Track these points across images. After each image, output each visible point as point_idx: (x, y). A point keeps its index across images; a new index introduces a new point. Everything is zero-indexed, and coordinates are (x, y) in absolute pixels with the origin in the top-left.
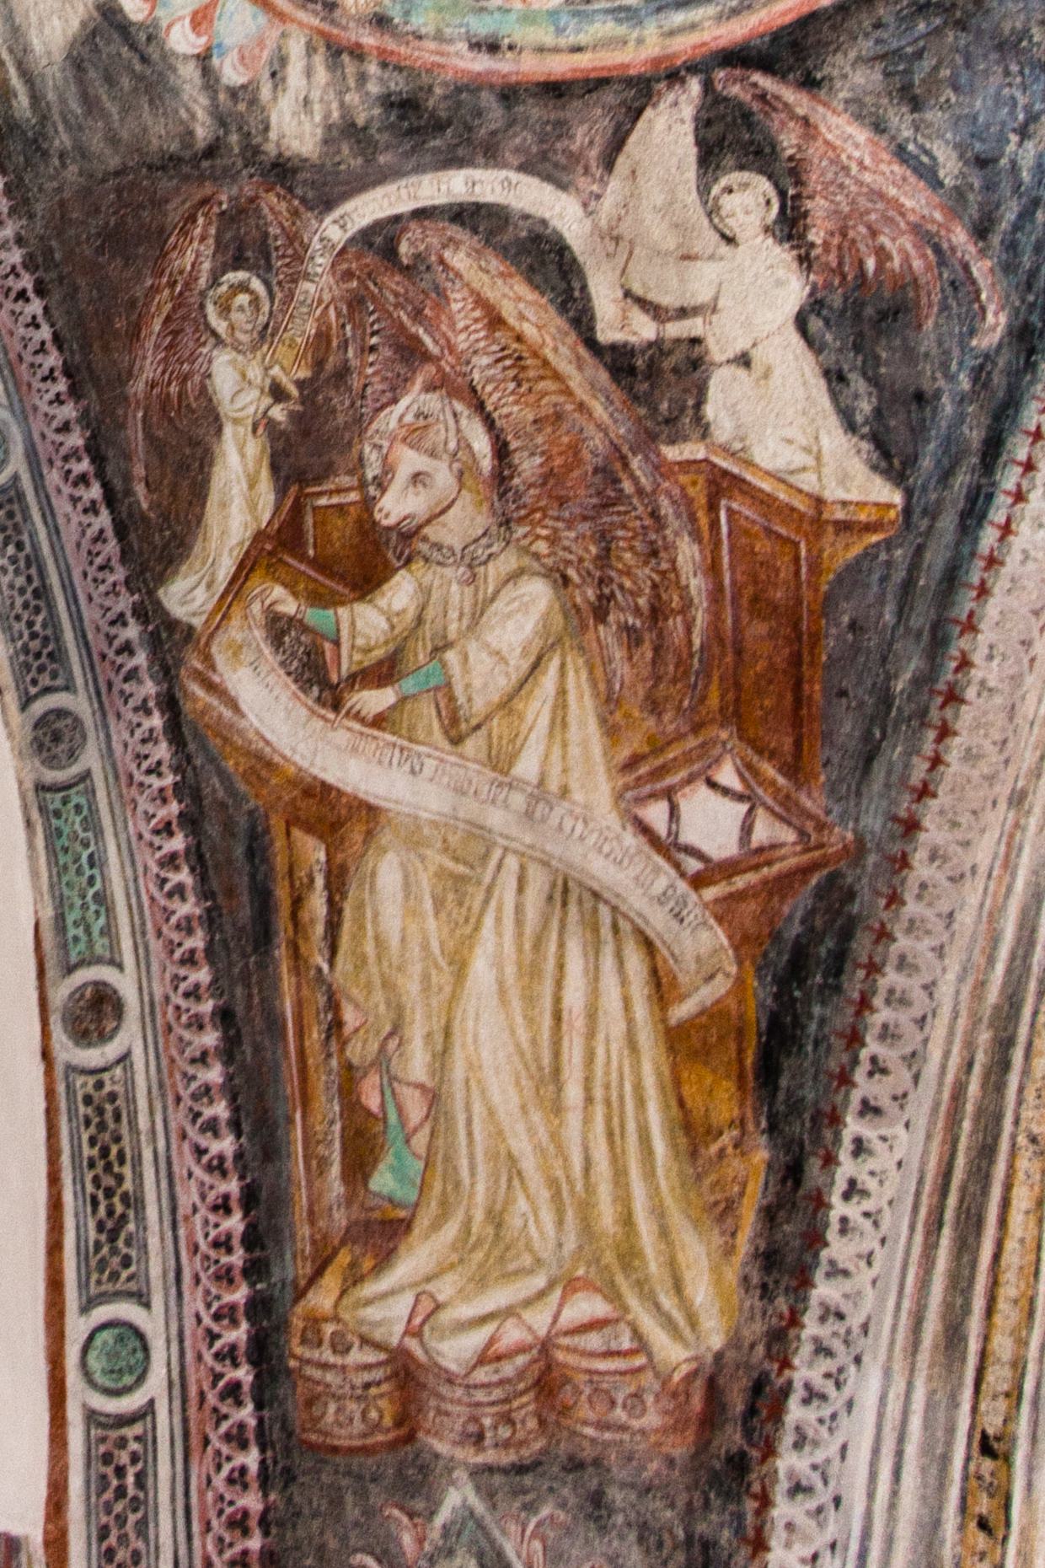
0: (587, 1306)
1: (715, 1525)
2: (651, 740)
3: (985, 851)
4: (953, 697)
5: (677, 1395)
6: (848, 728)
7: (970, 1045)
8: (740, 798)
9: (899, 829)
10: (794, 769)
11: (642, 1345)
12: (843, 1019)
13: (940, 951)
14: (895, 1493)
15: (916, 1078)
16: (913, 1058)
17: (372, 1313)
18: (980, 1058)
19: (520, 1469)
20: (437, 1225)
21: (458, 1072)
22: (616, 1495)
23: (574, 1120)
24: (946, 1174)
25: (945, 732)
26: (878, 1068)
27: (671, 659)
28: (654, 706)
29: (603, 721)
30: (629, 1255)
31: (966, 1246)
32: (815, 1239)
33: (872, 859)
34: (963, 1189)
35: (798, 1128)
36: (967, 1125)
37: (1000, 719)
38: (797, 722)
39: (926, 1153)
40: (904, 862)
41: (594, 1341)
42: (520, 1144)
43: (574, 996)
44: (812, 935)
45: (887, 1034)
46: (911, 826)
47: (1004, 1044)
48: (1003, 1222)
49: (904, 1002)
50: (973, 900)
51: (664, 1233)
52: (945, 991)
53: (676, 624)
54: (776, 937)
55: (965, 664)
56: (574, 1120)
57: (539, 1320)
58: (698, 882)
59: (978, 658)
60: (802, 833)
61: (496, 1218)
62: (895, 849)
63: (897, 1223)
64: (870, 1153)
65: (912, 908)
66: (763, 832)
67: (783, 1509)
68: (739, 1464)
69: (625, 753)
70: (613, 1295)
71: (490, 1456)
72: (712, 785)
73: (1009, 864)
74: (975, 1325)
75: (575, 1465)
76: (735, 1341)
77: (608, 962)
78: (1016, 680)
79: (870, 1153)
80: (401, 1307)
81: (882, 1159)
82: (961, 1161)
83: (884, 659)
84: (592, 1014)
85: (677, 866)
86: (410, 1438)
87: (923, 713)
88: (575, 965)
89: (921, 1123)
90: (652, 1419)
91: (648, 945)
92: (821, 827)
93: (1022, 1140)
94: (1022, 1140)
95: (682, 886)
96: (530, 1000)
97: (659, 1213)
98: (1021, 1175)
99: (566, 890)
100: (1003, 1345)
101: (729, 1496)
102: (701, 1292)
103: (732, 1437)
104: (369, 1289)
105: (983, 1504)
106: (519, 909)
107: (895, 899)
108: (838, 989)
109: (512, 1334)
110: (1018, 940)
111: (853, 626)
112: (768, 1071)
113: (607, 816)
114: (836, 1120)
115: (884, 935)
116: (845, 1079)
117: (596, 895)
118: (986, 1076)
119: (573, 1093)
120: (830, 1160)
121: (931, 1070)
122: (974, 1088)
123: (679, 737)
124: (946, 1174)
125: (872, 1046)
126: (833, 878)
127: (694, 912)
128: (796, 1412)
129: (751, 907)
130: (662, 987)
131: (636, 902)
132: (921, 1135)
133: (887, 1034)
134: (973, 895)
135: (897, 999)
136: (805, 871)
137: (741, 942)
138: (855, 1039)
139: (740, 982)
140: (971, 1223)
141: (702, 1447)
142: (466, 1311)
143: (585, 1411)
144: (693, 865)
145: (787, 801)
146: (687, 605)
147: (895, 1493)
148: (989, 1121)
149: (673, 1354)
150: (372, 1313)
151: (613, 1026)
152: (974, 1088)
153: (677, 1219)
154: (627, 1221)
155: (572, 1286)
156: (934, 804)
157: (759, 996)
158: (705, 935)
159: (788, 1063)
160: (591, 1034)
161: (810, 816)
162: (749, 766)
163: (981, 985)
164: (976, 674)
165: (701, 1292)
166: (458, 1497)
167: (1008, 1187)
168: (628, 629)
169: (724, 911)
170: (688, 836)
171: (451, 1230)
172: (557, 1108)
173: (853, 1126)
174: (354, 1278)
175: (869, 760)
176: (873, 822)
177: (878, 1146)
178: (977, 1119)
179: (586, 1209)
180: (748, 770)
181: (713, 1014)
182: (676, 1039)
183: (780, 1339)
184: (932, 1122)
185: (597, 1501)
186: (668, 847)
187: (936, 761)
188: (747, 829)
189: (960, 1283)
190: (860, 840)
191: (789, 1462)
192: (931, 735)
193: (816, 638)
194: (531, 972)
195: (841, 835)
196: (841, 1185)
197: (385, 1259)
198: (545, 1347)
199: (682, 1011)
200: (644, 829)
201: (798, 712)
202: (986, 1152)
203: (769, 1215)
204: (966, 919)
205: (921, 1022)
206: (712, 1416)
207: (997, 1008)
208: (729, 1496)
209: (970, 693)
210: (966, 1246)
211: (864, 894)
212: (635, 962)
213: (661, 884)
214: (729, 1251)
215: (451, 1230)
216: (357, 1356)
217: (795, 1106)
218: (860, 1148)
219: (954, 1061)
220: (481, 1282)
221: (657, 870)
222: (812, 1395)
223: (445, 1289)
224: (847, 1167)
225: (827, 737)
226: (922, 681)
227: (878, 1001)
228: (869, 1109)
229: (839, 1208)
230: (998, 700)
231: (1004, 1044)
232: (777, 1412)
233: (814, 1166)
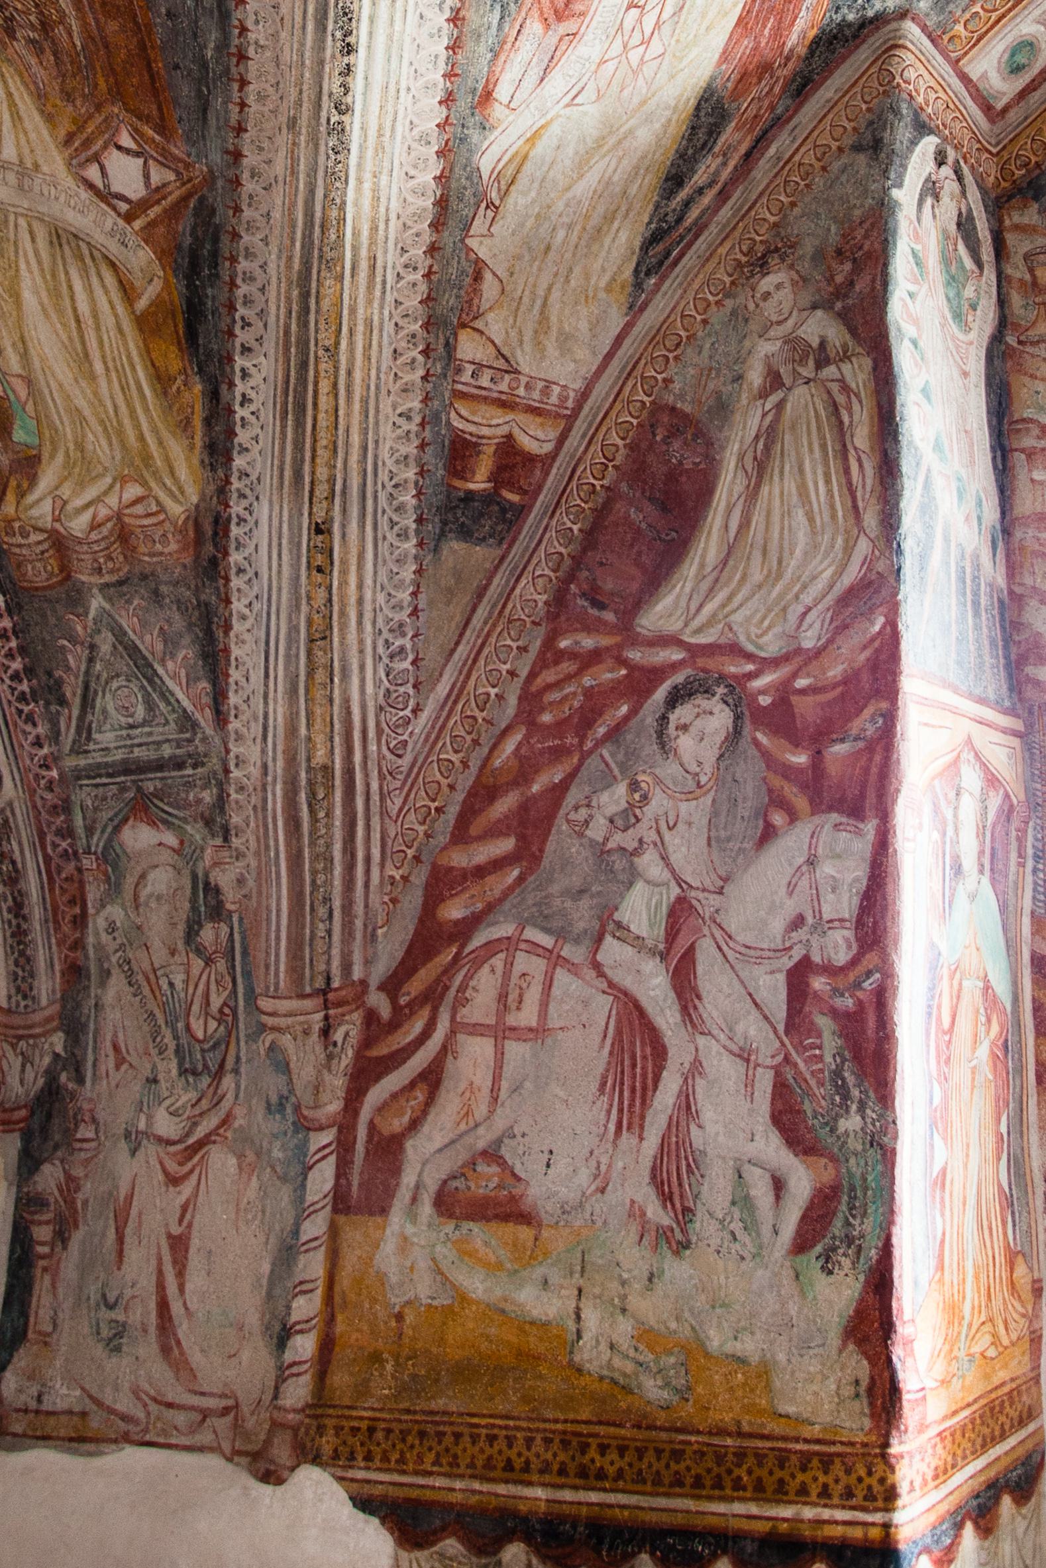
0: (133, 491)
1: (208, 595)
2: (74, 121)
3: (280, 167)
4: (242, 57)
5: (182, 531)
6: (186, 90)
7: (289, 299)
8: (137, 154)
9: (230, 159)
10: (162, 129)
11: (162, 509)
12: (223, 297)
13: (265, 241)
14: (280, 565)
15: (265, 325)
16: (262, 314)
17: (35, 512)
18: (295, 307)
19: (121, 583)
20: (52, 457)
21: (37, 364)
22: (164, 589)
23: (103, 383)
24: (287, 382)
25: (243, 83)
26: (246, 324)
27: (66, 59)
28: (68, 96)
29: (42, 112)
30: (147, 459)
31: (299, 424)
32: (231, 433)
33: (220, 183)
34: (295, 390)
35: (212, 369)
36: (293, 350)
37: (270, 68)
38: (155, 92)
39: (276, 370)
40: (237, 182)
41: (139, 509)
42: (81, 402)
43: (83, 307)
44: (198, 242)
45: (247, 301)
46: (237, 155)
47: (305, 296)
48: (315, 405)
49: (252, 279)
50: (279, 202)
51: (160, 443)
52: (272, 268)
53: (60, 31)
54: (179, 247)
55: (244, 30)
56: (103, 383)
57: (113, 501)
58: (129, 218)
59: (250, 24)
60: (178, 173)
61: (80, 447)
62: (230, 174)
63: (267, 415)
64: (250, 376)
65: (247, 213)
66: (158, 176)
67: (236, 582)
68: (214, 562)
69: (62, 133)
70: (144, 484)
71: (107, 578)
72: (119, 148)
73: (294, 172)
74: (307, 468)
75: (144, 577)
76: (203, 497)
77: (95, 280)
78: (275, 36)
79: (250, 376)
80: (46, 507)
81: (256, 379)
82: (293, 373)
83: (195, 35)
84: (95, 315)
85: (114, 209)
86: (68, 577)
87: (227, 71)
88: (78, 286)
89: (272, 352)
90: (173, 546)
91: (113, 265)
92: (187, 166)
93: (321, 353)
94: (321, 353)
95: (121, 222)
96: (60, 312)
97: (155, 430)
98: (323, 374)
99: (58, 237)
100: (322, 473)
101: (213, 579)
102: (183, 473)
103: (209, 549)
104: (31, 498)
105: (319, 560)
106: (37, 253)
107: (237, 210)
108: (217, 276)
109: (103, 512)
110: (305, 224)
111: (170, 15)
112: (192, 335)
113: (69, 182)
114: (230, 360)
115: (236, 236)
116: (231, 334)
117: (75, 236)
118: (299, 318)
119: (99, 367)
120: (231, 385)
121: (272, 319)
122: (294, 327)
123: (91, 117)
124: (287, 382)
125: (241, 311)
126: (202, 199)
127: (132, 240)
128: (235, 531)
129: (161, 230)
130: (128, 292)
131: (99, 238)
132: (273, 360)
133: (247, 301)
134: (278, 198)
135: (249, 278)
136: (185, 199)
137: (161, 255)
138: (232, 308)
139: (166, 281)
140: (301, 408)
141: (197, 557)
142: (78, 502)
143: (142, 549)
144: (124, 207)
145: (164, 152)
146: (63, 16)
147: (280, 565)
148: (303, 344)
149: (176, 510)
150: (35, 512)
151: (108, 321)
152: (294, 327)
153: (165, 434)
154: (141, 438)
155: (123, 480)
156: (246, 136)
157: (179, 287)
158: (141, 253)
159: (201, 329)
160: (98, 329)
161: (181, 160)
162: (136, 130)
163: (290, 258)
164: (252, 36)
165: (183, 473)
166: (97, 603)
167: (316, 384)
168: (32, 41)
169: (147, 234)
170: (116, 188)
171: (60, 458)
172: (93, 377)
173: (240, 362)
174: (21, 495)
175: (205, 111)
176: (216, 157)
177: (253, 371)
178: (297, 347)
179: (120, 433)
180: (136, 133)
181: (156, 303)
182: (141, 321)
183: (222, 491)
184: (277, 352)
185: (156, 592)
186: (106, 196)
187: (243, 105)
188: (147, 176)
189: (298, 446)
190: (211, 171)
191: (235, 557)
192: (236, 86)
193: (149, 26)
194: (55, 293)
195: (201, 168)
196: (239, 398)
197: (33, 480)
198: (119, 516)
199: (142, 304)
200: (91, 186)
201: (154, 87)
202: (304, 365)
203: (208, 422)
204: (276, 215)
205: (262, 290)
206: (199, 541)
207: (300, 272)
208: (213, 579)
209: (251, 52)
210: (299, 424)
211: (220, 210)
212: (110, 279)
213: (109, 223)
214: (192, 447)
215: (60, 458)
216: (34, 537)
217: (209, 355)
218: (245, 374)
219: (283, 310)
220: (81, 485)
221: (104, 214)
222: (241, 520)
223: (66, 491)
224: (240, 387)
225: (176, 102)
226: (223, 45)
227: (239, 281)
228: (246, 350)
229: (240, 412)
230: (268, 54)
231: (305, 296)
232: (227, 531)
233: (224, 387)
